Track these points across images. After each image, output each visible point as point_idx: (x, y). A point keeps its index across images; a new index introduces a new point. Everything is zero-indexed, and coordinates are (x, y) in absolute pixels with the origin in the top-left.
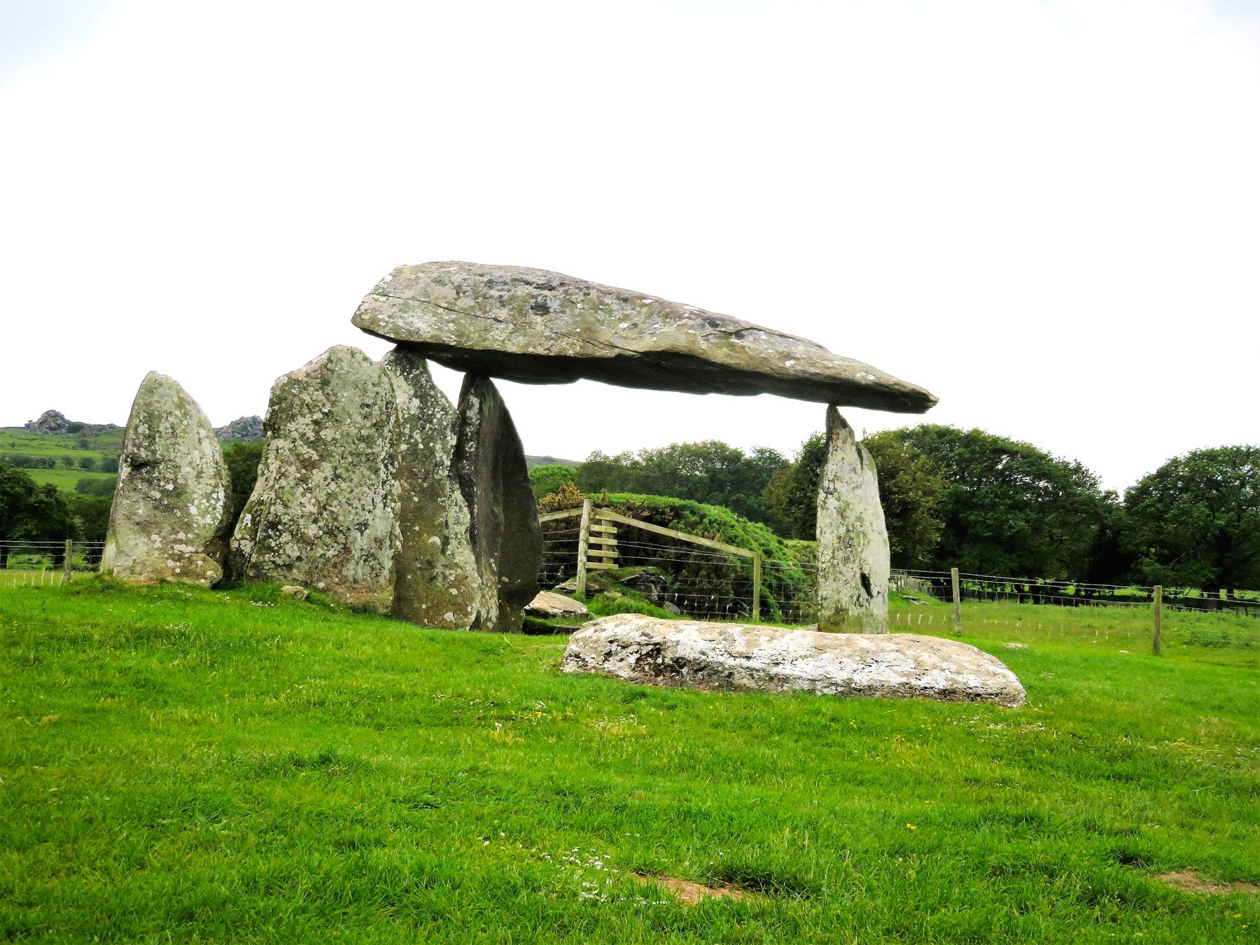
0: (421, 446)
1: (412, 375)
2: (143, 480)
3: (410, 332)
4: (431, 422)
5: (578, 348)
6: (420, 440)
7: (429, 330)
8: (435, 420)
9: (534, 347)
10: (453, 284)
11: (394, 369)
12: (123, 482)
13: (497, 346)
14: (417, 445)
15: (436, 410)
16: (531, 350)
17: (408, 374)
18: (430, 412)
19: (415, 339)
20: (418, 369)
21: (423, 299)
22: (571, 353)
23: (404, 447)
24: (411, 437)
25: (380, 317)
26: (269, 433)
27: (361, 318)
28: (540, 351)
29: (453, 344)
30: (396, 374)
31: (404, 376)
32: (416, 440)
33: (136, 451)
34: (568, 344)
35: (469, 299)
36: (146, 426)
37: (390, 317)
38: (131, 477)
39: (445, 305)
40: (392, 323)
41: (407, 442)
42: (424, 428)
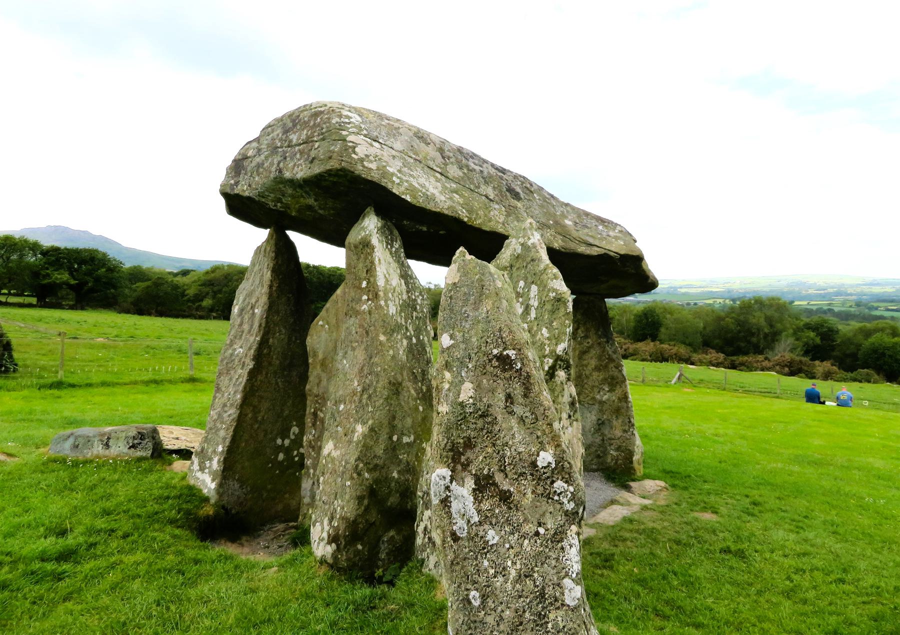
1: (394, 249)
3: (430, 198)
4: (415, 309)
8: (418, 307)
21: (414, 156)
23: (405, 342)
24: (407, 329)
25: (391, 170)
27: (363, 166)
29: (466, 220)
35: (455, 166)
37: (400, 171)
39: (440, 170)
40: (407, 181)
42: (412, 317)
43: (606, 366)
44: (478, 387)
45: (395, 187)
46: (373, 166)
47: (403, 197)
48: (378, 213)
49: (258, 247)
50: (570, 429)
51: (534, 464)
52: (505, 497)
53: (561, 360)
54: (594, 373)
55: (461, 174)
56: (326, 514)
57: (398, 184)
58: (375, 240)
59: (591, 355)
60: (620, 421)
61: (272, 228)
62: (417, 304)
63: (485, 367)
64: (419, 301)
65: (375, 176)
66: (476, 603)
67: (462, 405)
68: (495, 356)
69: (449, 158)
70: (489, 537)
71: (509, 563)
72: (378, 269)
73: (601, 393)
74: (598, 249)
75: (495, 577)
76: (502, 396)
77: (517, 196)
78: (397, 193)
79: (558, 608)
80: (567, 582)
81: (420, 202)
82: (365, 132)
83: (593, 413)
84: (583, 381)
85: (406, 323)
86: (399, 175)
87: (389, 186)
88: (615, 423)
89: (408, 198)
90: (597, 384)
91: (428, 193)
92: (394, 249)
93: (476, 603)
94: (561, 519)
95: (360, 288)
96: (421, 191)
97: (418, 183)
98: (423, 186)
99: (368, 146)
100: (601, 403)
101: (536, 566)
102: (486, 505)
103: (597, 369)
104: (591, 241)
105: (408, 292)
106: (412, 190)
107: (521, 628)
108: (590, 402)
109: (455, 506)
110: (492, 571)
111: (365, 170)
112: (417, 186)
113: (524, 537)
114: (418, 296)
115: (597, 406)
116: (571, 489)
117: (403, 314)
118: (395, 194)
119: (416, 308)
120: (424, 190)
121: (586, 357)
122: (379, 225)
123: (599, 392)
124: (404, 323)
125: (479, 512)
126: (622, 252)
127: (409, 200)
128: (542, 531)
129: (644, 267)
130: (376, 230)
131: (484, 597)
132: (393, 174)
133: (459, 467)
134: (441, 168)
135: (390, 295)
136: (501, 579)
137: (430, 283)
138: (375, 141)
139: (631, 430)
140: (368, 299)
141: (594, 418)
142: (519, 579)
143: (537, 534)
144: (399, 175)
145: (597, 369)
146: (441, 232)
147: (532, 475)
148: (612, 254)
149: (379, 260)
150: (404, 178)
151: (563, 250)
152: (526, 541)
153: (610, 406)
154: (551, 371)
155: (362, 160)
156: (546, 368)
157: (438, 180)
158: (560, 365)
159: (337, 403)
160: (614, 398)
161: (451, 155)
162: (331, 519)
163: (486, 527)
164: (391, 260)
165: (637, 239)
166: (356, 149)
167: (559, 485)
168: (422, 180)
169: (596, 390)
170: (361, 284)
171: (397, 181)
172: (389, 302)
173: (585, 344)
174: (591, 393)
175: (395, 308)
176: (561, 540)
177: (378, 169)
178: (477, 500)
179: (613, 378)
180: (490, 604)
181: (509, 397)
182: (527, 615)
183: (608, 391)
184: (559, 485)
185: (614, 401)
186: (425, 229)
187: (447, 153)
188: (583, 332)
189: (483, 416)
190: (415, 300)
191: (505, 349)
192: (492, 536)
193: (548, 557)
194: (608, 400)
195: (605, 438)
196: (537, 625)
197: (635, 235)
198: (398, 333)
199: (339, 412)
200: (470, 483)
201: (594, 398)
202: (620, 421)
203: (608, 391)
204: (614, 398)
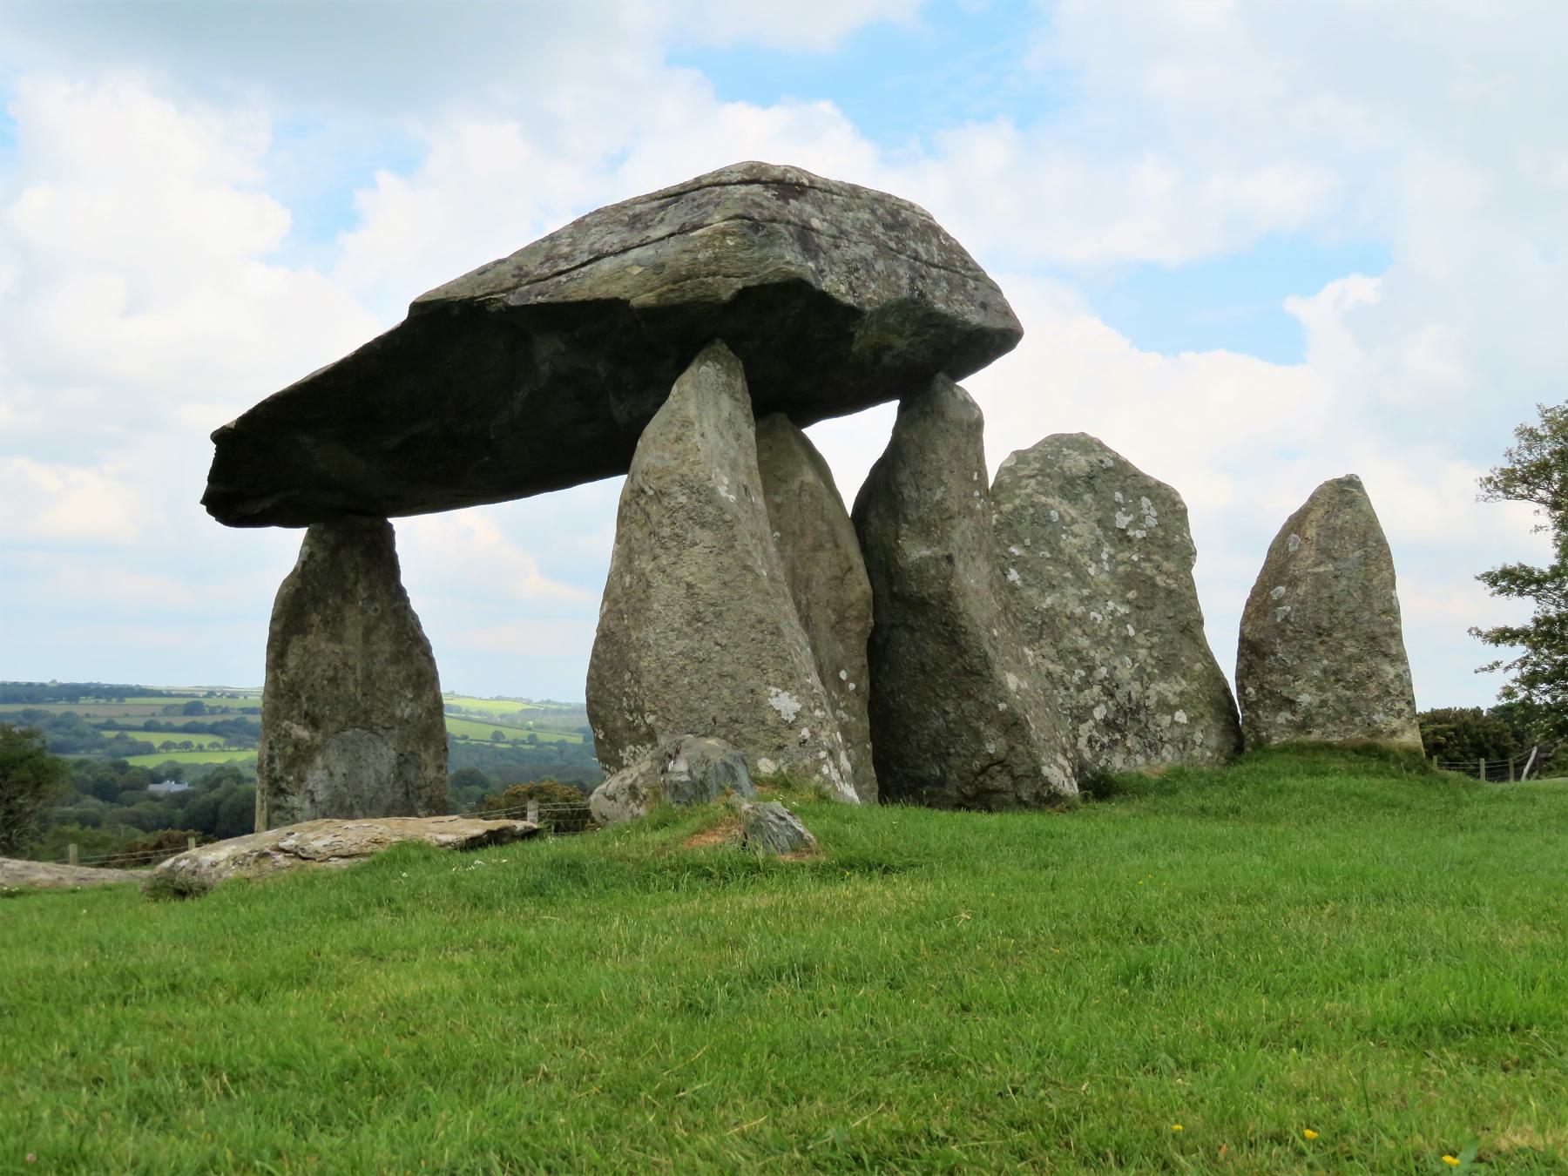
43: (408, 654)
54: (389, 669)
56: (1055, 751)
60: (432, 751)
61: (721, 347)
73: (403, 704)
83: (391, 744)
84: (374, 684)
88: (423, 755)
90: (397, 688)
95: (970, 480)
100: (404, 722)
103: (395, 659)
108: (387, 725)
115: (396, 732)
121: (374, 638)
141: (393, 753)
145: (395, 659)
153: (415, 726)
159: (988, 630)
160: (419, 710)
162: (1065, 754)
169: (396, 698)
170: (972, 475)
173: (371, 612)
174: (388, 706)
179: (420, 674)
185: (420, 717)
188: (365, 589)
194: (411, 716)
195: (411, 788)
199: (995, 639)
201: (392, 716)
202: (432, 751)
203: (411, 700)
204: (419, 710)
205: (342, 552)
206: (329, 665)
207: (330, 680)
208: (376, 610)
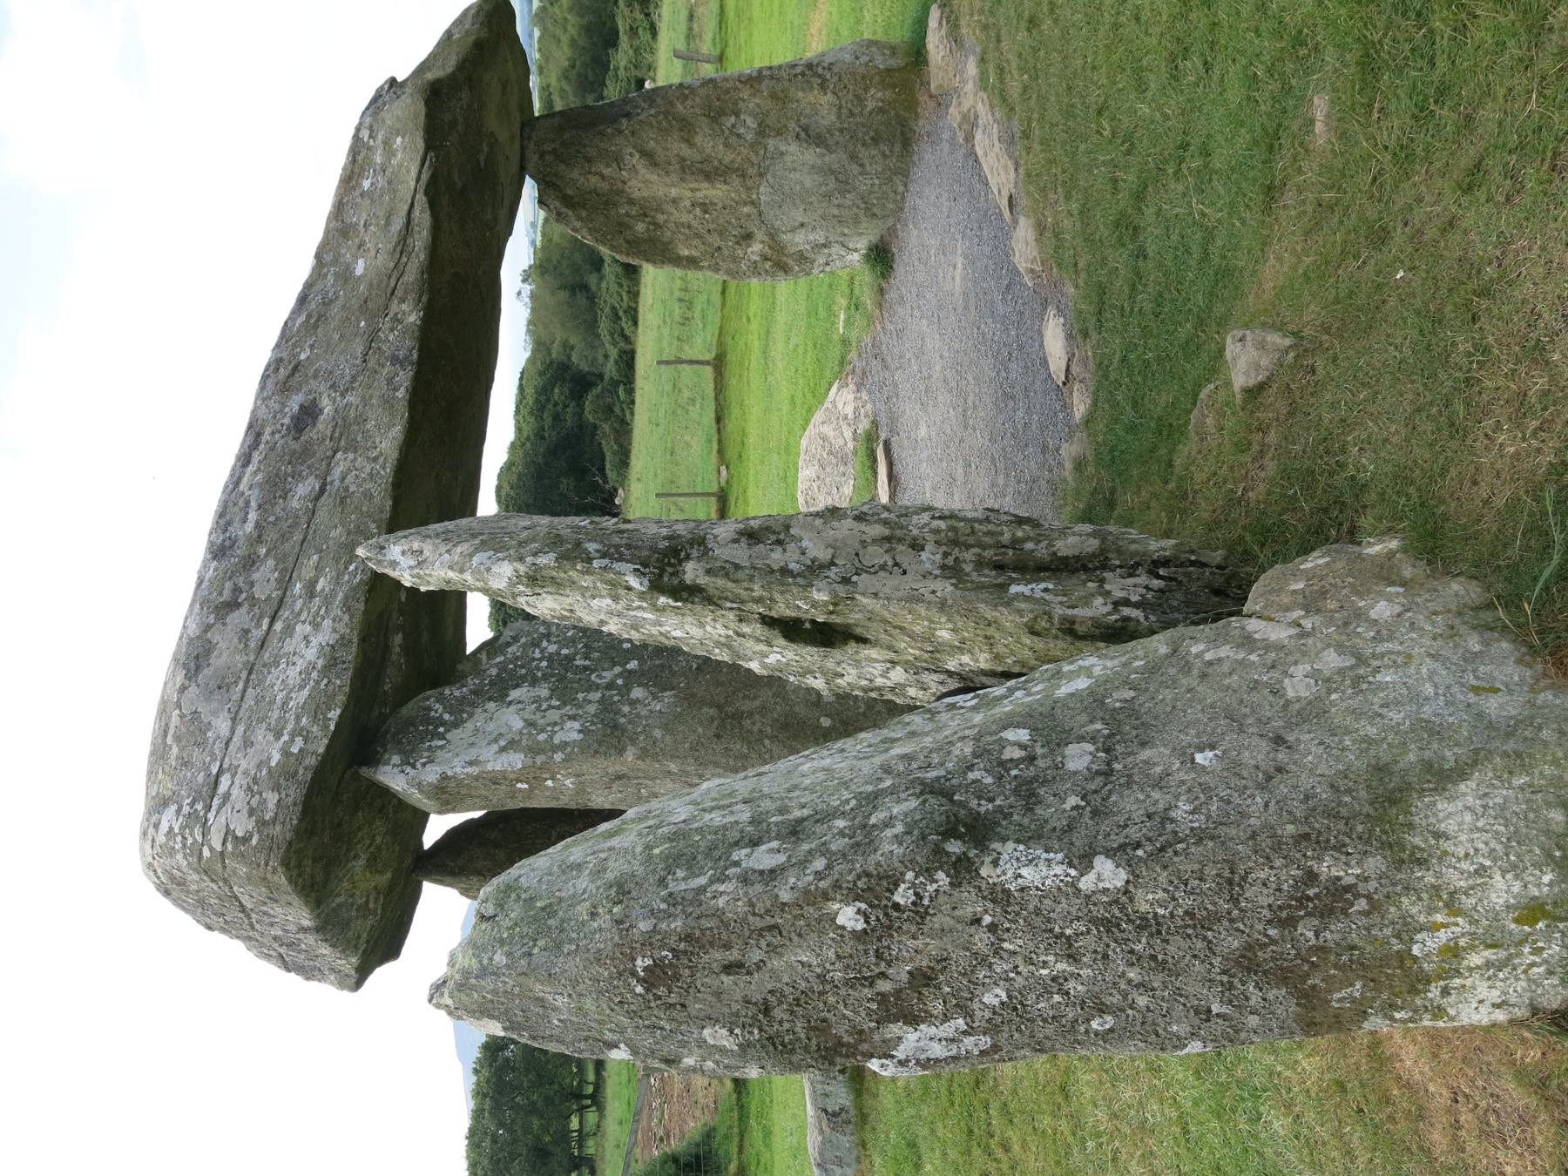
0: (633, 665)
1: (447, 717)
2: (1028, 793)
3: (331, 664)
4: (570, 659)
5: (404, 307)
6: (618, 669)
7: (327, 623)
8: (565, 651)
9: (396, 389)
10: (208, 628)
11: (425, 754)
12: (1084, 861)
13: (387, 471)
14: (631, 672)
15: (537, 655)
16: (401, 394)
17: (443, 723)
18: (544, 664)
19: (350, 655)
20: (429, 709)
21: (241, 686)
22: (413, 318)
23: (637, 693)
24: (611, 686)
25: (276, 758)
26: (692, 571)
27: (274, 820)
28: (404, 377)
30: (441, 747)
31: (447, 731)
32: (620, 675)
33: (899, 828)
34: (392, 330)
36: (739, 854)
37: (278, 735)
38: (1033, 836)
39: (266, 622)
40: (298, 718)
41: (627, 687)
42: (586, 668)
44: (712, 1020)
45: (311, 748)
46: (272, 798)
47: (332, 728)
48: (374, 760)
49: (462, 894)
50: (805, 544)
51: (859, 936)
52: (923, 979)
53: (662, 571)
55: (271, 563)
57: (306, 741)
58: (431, 775)
59: (659, 150)
62: (558, 654)
63: (672, 1006)
64: (552, 648)
65: (294, 793)
66: (1110, 1021)
67: (745, 1047)
68: (647, 990)
69: (237, 590)
70: (996, 1002)
71: (1044, 972)
72: (489, 767)
73: (742, 131)
74: (416, 213)
75: (1068, 993)
76: (727, 980)
77: (309, 413)
78: (326, 741)
79: (1131, 900)
80: (1087, 883)
81: (342, 682)
82: (199, 806)
83: (783, 148)
85: (598, 687)
86: (286, 738)
87: (311, 761)
89: (334, 714)
91: (320, 663)
92: (447, 717)
93: (1110, 1021)
94: (967, 894)
96: (318, 683)
97: (302, 687)
98: (307, 673)
99: (228, 807)
101: (1051, 931)
102: (938, 1007)
104: (398, 224)
105: (534, 682)
106: (316, 710)
107: (1160, 957)
109: (937, 1050)
110: (1057, 998)
111: (281, 817)
112: (306, 692)
113: (997, 952)
114: (542, 651)
116: (910, 875)
117: (580, 696)
118: (328, 747)
119: (566, 656)
120: (314, 675)
122: (396, 759)
123: (739, 136)
124: (598, 695)
125: (946, 1018)
126: (421, 145)
127: (339, 711)
128: (987, 919)
129: (450, 66)
130: (408, 769)
131: (1102, 1010)
132: (286, 753)
133: (864, 1047)
134: (261, 617)
135: (542, 737)
136: (1071, 984)
137: (519, 293)
138: (216, 783)
139: (820, 71)
140: (553, 778)
141: (793, 147)
142: (1073, 958)
143: (992, 928)
144: (286, 738)
146: (403, 599)
147: (880, 939)
148: (425, 177)
149: (471, 763)
150: (290, 727)
151: (424, 299)
152: (1006, 945)
154: (685, 595)
155: (262, 824)
156: (679, 604)
157: (289, 630)
158: (672, 574)
161: (228, 585)
163: (976, 1006)
164: (469, 725)
165: (387, 76)
166: (240, 834)
167: (902, 896)
168: (293, 673)
171: (299, 742)
172: (556, 741)
175: (569, 725)
176: (1007, 892)
177: (277, 788)
178: (928, 1018)
180: (1116, 999)
181: (729, 968)
182: (1138, 947)
183: (737, 116)
184: (902, 896)
186: (398, 639)
187: (227, 595)
189: (767, 1010)
190: (550, 659)
191: (634, 974)
192: (994, 997)
193: (1038, 912)
196: (1159, 932)
197: (380, 80)
198: (617, 712)
200: (895, 1029)
201: (753, 146)
205: (569, 192)
206: (690, 212)
207: (706, 212)
208: (631, 155)
